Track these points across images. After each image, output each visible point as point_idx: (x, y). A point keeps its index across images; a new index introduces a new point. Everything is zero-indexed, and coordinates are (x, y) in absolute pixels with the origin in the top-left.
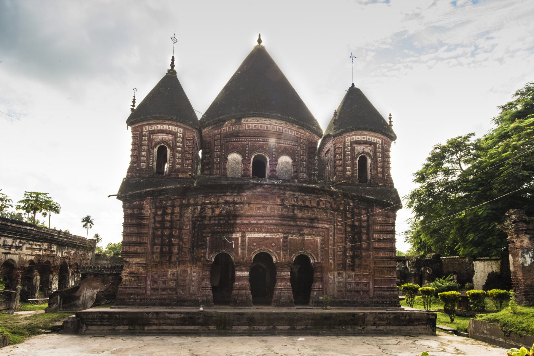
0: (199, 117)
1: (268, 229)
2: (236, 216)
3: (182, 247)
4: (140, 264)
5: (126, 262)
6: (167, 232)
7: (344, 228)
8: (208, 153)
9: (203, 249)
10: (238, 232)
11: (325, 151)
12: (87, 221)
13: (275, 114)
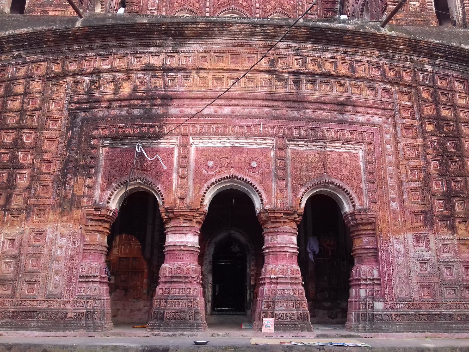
1: (241, 127)
2: (168, 99)
3: (40, 173)
7: (417, 123)
9: (89, 175)
10: (172, 135)
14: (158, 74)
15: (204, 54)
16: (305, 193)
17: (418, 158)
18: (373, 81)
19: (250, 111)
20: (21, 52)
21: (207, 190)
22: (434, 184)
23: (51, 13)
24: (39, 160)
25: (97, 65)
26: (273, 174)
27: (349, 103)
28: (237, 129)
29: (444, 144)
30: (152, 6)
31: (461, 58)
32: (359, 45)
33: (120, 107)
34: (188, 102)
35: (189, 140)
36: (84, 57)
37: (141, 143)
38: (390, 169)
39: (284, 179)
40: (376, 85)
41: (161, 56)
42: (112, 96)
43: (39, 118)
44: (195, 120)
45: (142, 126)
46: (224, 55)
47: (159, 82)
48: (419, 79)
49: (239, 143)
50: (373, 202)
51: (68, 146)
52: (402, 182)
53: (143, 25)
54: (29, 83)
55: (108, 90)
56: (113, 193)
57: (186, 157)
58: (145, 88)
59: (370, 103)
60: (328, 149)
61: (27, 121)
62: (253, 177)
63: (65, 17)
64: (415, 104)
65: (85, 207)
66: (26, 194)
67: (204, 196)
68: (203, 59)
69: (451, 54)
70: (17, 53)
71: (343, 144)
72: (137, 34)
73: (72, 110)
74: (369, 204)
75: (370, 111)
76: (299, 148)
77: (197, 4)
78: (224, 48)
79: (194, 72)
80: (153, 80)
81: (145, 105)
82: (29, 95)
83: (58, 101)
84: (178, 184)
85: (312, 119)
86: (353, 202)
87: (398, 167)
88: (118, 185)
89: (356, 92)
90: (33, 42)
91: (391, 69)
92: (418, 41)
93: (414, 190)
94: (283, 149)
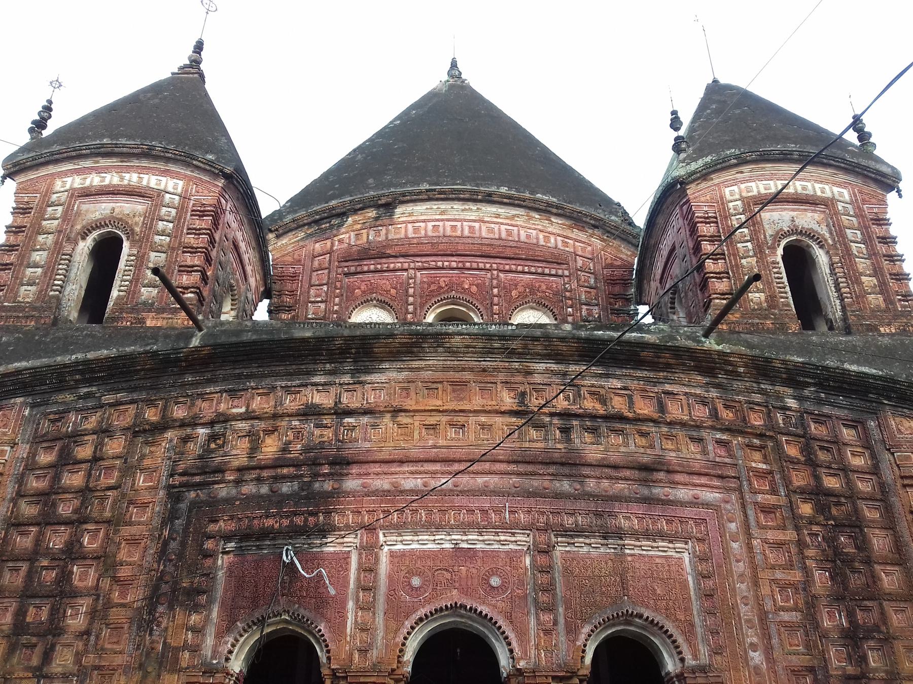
1: (471, 511)
2: (342, 463)
3: (108, 605)
6: (57, 540)
7: (783, 501)
8: (290, 309)
9: (196, 608)
11: (660, 271)
13: (493, 189)
14: (327, 420)
15: (406, 385)
16: (590, 636)
17: (790, 566)
18: (698, 427)
19: (486, 482)
20: (94, 389)
21: (409, 633)
22: (825, 616)
23: (149, 323)
24: (108, 581)
25: (223, 407)
26: (530, 599)
27: (659, 467)
28: (464, 517)
29: (835, 539)
30: (316, 296)
31: (845, 386)
32: (667, 367)
33: (259, 480)
34: (377, 468)
35: (378, 537)
36: (201, 396)
37: (293, 545)
38: (742, 587)
39: (550, 608)
40: (704, 434)
41: (333, 390)
42: (243, 461)
43: (115, 502)
44: (389, 501)
45: (295, 514)
46: (439, 386)
47: (328, 434)
48: (777, 421)
49: (467, 540)
50: (717, 651)
51: (162, 553)
52: (766, 613)
53: (304, 340)
54: (103, 440)
55: (238, 451)
56: (237, 641)
57: (371, 570)
58: (303, 446)
59: (697, 467)
60: (627, 551)
61: (93, 510)
62: (495, 606)
63: (173, 328)
64: (775, 468)
65: (187, 668)
66: (80, 645)
67: (404, 644)
68: (404, 394)
69: (827, 380)
70: (86, 390)
71: (654, 541)
72: (293, 356)
73: (174, 487)
74: (709, 655)
75: (696, 480)
76: (576, 549)
77: (393, 291)
78: (439, 375)
79: (388, 415)
80: (317, 432)
81: (302, 476)
82: (102, 463)
83: (150, 471)
84: (356, 621)
85: (597, 496)
86: (680, 653)
87: (756, 583)
88: (248, 624)
89: (670, 447)
90: (118, 373)
91: (727, 407)
92: (768, 360)
93: (790, 627)
94: (547, 551)
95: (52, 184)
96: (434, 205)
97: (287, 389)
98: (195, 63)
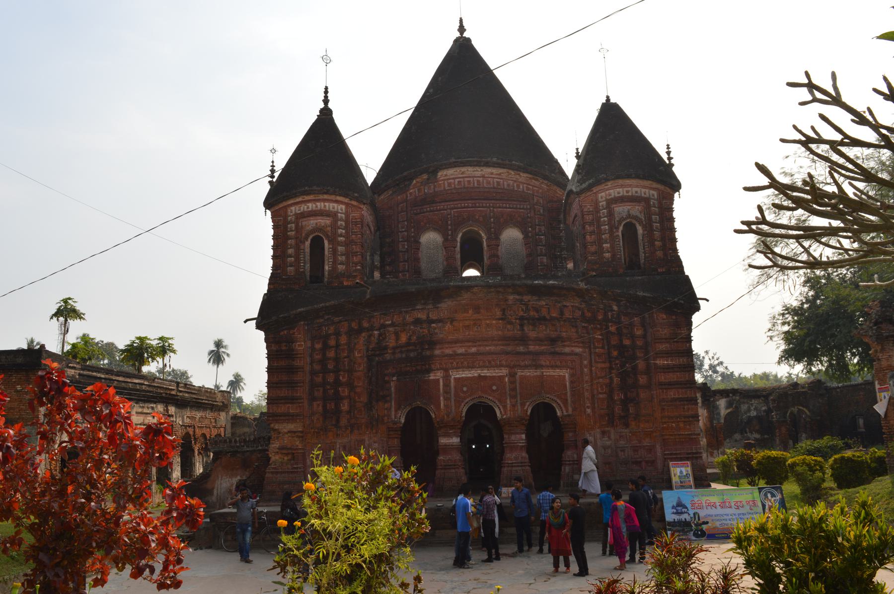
0: (370, 176)
1: (484, 362)
2: (432, 344)
4: (295, 432)
5: (275, 430)
6: (331, 378)
10: (438, 370)
12: (217, 357)
23: (345, 284)
30: (403, 228)
33: (401, 352)
50: (574, 409)
83: (359, 352)
95: (286, 212)
96: (458, 169)
97: (406, 312)
98: (326, 101)
